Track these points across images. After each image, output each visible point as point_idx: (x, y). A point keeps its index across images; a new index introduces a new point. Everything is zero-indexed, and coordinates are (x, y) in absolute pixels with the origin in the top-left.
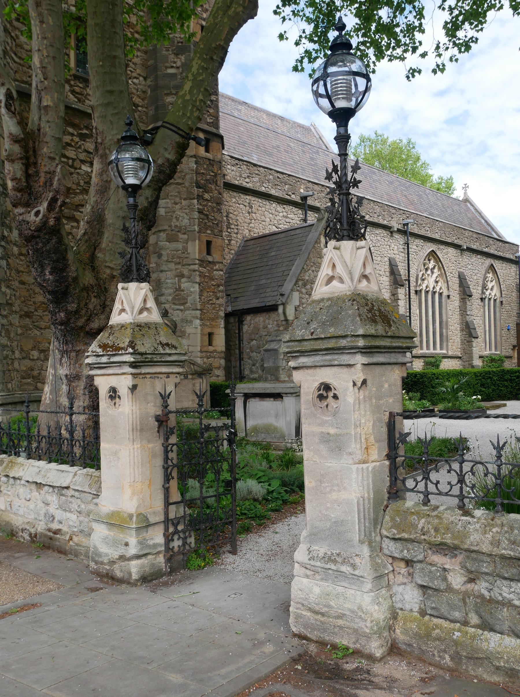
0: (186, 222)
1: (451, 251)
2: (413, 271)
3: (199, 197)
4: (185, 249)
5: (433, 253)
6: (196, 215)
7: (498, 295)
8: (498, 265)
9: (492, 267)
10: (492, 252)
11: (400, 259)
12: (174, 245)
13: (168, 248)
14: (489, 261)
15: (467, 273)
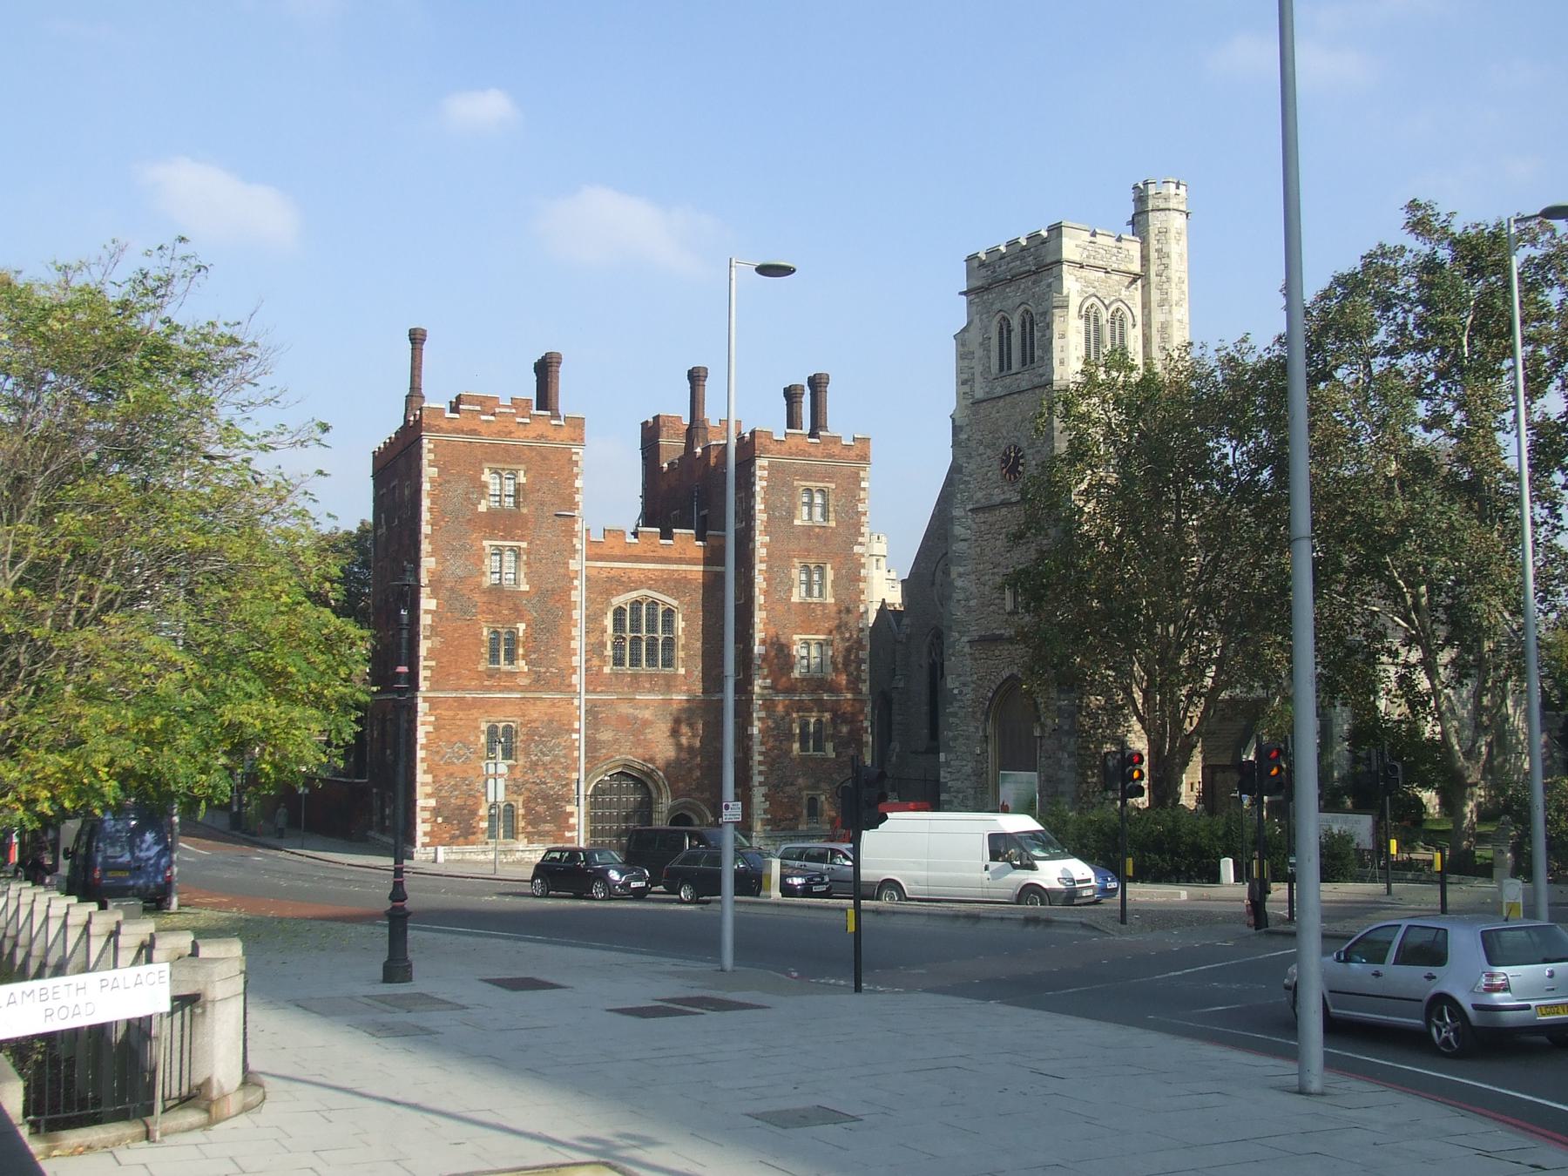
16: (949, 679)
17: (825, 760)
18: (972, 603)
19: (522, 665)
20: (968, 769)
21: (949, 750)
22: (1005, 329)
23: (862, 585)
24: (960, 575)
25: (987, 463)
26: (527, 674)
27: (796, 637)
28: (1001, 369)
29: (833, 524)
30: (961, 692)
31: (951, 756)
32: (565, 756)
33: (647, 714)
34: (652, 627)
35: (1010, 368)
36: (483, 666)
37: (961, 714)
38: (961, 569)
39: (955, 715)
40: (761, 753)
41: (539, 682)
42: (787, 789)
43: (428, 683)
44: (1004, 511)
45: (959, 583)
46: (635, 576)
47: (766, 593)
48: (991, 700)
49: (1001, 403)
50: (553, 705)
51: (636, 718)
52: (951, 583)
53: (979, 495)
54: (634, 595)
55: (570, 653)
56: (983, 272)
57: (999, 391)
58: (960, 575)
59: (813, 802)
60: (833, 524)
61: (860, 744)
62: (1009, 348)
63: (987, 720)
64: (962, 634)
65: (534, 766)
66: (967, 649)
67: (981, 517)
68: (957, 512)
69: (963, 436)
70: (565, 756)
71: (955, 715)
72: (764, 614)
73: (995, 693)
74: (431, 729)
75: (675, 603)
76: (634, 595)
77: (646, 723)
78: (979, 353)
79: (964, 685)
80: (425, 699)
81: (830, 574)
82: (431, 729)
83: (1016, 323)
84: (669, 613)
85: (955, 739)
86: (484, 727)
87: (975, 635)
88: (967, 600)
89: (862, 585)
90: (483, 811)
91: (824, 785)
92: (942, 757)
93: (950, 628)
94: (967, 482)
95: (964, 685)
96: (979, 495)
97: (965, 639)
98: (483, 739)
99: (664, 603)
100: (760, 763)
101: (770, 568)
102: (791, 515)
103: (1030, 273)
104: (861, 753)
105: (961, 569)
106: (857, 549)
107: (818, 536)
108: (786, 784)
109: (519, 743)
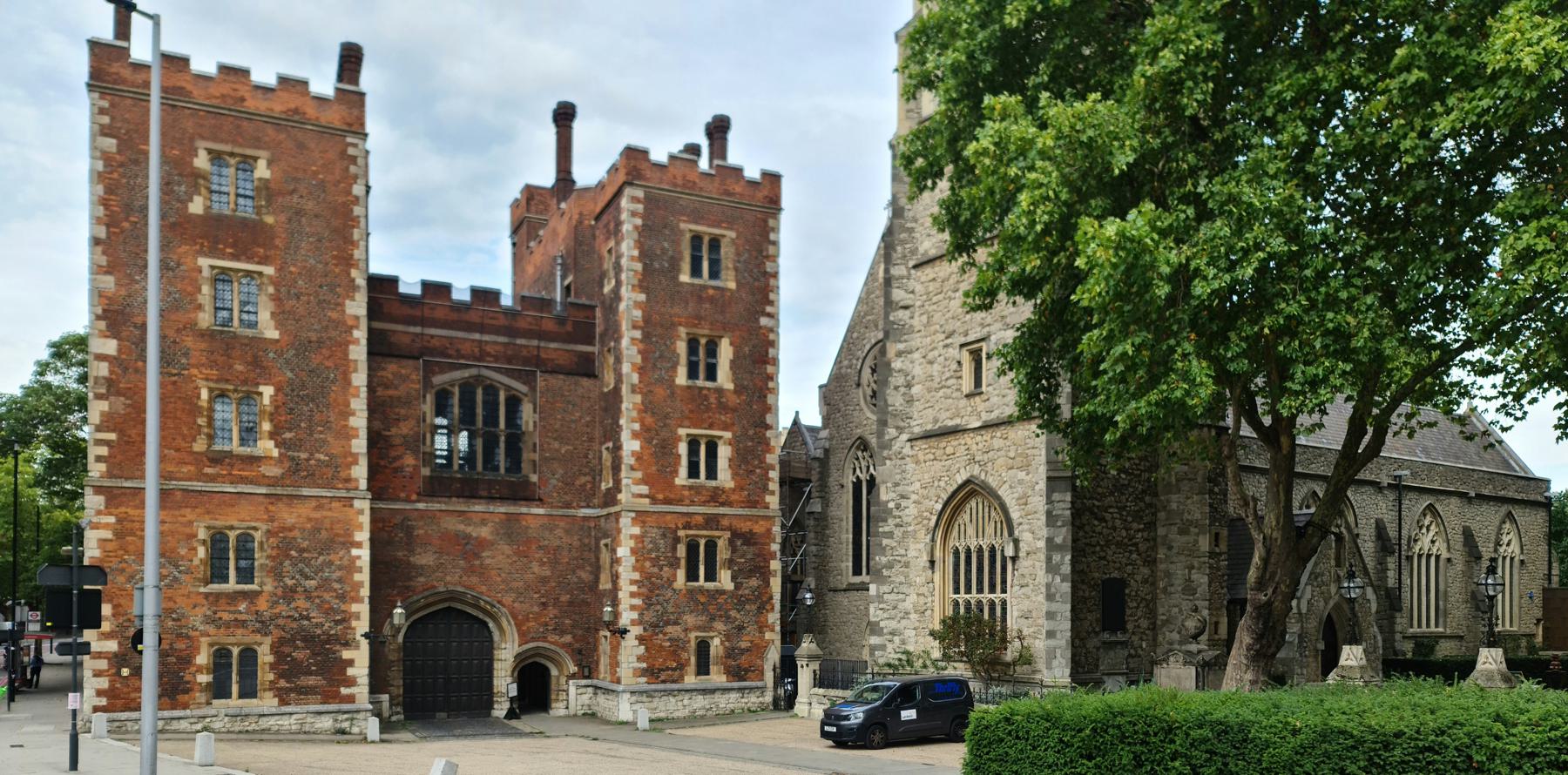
0: (1198, 516)
1: (1454, 500)
2: (1404, 532)
3: (1211, 492)
4: (1196, 542)
5: (1431, 507)
6: (1207, 509)
7: (1517, 551)
8: (1517, 512)
9: (1510, 515)
10: (1511, 494)
11: (1389, 518)
12: (1185, 539)
13: (1179, 541)
14: (1504, 509)
15: (1474, 527)
16: (882, 489)
17: (722, 592)
18: (915, 390)
19: (266, 447)
23: (770, 369)
24: (899, 354)
26: (280, 460)
27: (682, 432)
29: (732, 285)
30: (898, 507)
31: (885, 588)
32: (340, 581)
33: (485, 532)
34: (491, 419)
36: (200, 446)
37: (898, 532)
38: (901, 346)
39: (890, 535)
40: (633, 582)
41: (296, 471)
42: (669, 629)
43: (103, 467)
45: (897, 364)
46: (466, 348)
47: (641, 370)
50: (319, 507)
51: (468, 537)
52: (888, 364)
54: (466, 373)
55: (348, 434)
58: (899, 354)
59: (703, 648)
60: (732, 285)
61: (765, 574)
64: (900, 430)
65: (289, 594)
66: (907, 450)
70: (340, 581)
71: (890, 535)
72: (638, 398)
74: (108, 535)
75: (524, 388)
76: (466, 373)
77: (482, 544)
79: (903, 497)
80: (98, 490)
81: (725, 351)
82: (108, 535)
84: (514, 403)
85: (890, 566)
86: (202, 534)
87: (917, 430)
88: (909, 386)
89: (770, 369)
90: (202, 659)
91: (720, 626)
95: (903, 497)
97: (905, 437)
98: (202, 552)
99: (508, 388)
100: (633, 595)
101: (647, 337)
102: (675, 268)
104: (768, 584)
105: (901, 346)
106: (764, 321)
107: (712, 300)
108: (667, 623)
109: (260, 559)
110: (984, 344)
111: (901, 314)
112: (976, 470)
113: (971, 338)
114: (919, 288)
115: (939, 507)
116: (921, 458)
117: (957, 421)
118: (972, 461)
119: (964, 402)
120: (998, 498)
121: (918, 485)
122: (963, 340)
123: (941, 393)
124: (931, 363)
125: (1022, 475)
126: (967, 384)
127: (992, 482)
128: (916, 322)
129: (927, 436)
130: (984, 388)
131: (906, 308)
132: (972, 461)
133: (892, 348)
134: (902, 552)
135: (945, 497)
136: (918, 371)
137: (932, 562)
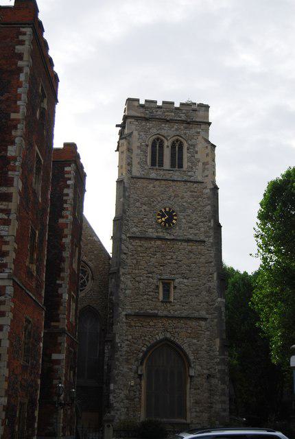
20: (122, 395)
21: (115, 383)
22: (157, 145)
25: (143, 213)
28: (153, 164)
35: (161, 164)
44: (159, 242)
45: (122, 279)
48: (145, 354)
49: (157, 183)
52: (119, 278)
53: (134, 229)
56: (142, 110)
57: (153, 175)
58: (123, 274)
62: (161, 155)
63: (142, 364)
64: (123, 309)
67: (138, 242)
68: (124, 237)
69: (127, 194)
73: (149, 349)
78: (136, 151)
83: (167, 144)
85: (118, 375)
87: (129, 312)
92: (112, 386)
93: (118, 305)
94: (127, 220)
96: (134, 229)
97: (124, 313)
103: (183, 122)
110: (172, 282)
111: (124, 256)
112: (168, 335)
113: (165, 277)
114: (130, 247)
115: (145, 349)
116: (133, 324)
117: (156, 312)
118: (166, 330)
119: (160, 304)
120: (182, 350)
121: (130, 337)
122: (159, 277)
123: (145, 297)
124: (139, 282)
125: (195, 341)
126: (161, 298)
127: (179, 342)
128: (129, 261)
129: (137, 315)
130: (172, 299)
131: (125, 254)
132: (166, 330)
133: (122, 271)
134: (122, 369)
135: (149, 345)
136: (129, 283)
137: (140, 376)
